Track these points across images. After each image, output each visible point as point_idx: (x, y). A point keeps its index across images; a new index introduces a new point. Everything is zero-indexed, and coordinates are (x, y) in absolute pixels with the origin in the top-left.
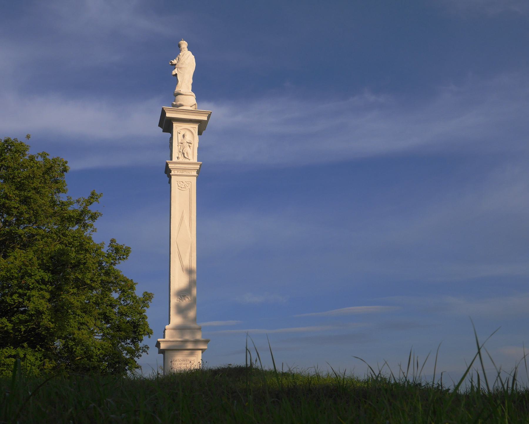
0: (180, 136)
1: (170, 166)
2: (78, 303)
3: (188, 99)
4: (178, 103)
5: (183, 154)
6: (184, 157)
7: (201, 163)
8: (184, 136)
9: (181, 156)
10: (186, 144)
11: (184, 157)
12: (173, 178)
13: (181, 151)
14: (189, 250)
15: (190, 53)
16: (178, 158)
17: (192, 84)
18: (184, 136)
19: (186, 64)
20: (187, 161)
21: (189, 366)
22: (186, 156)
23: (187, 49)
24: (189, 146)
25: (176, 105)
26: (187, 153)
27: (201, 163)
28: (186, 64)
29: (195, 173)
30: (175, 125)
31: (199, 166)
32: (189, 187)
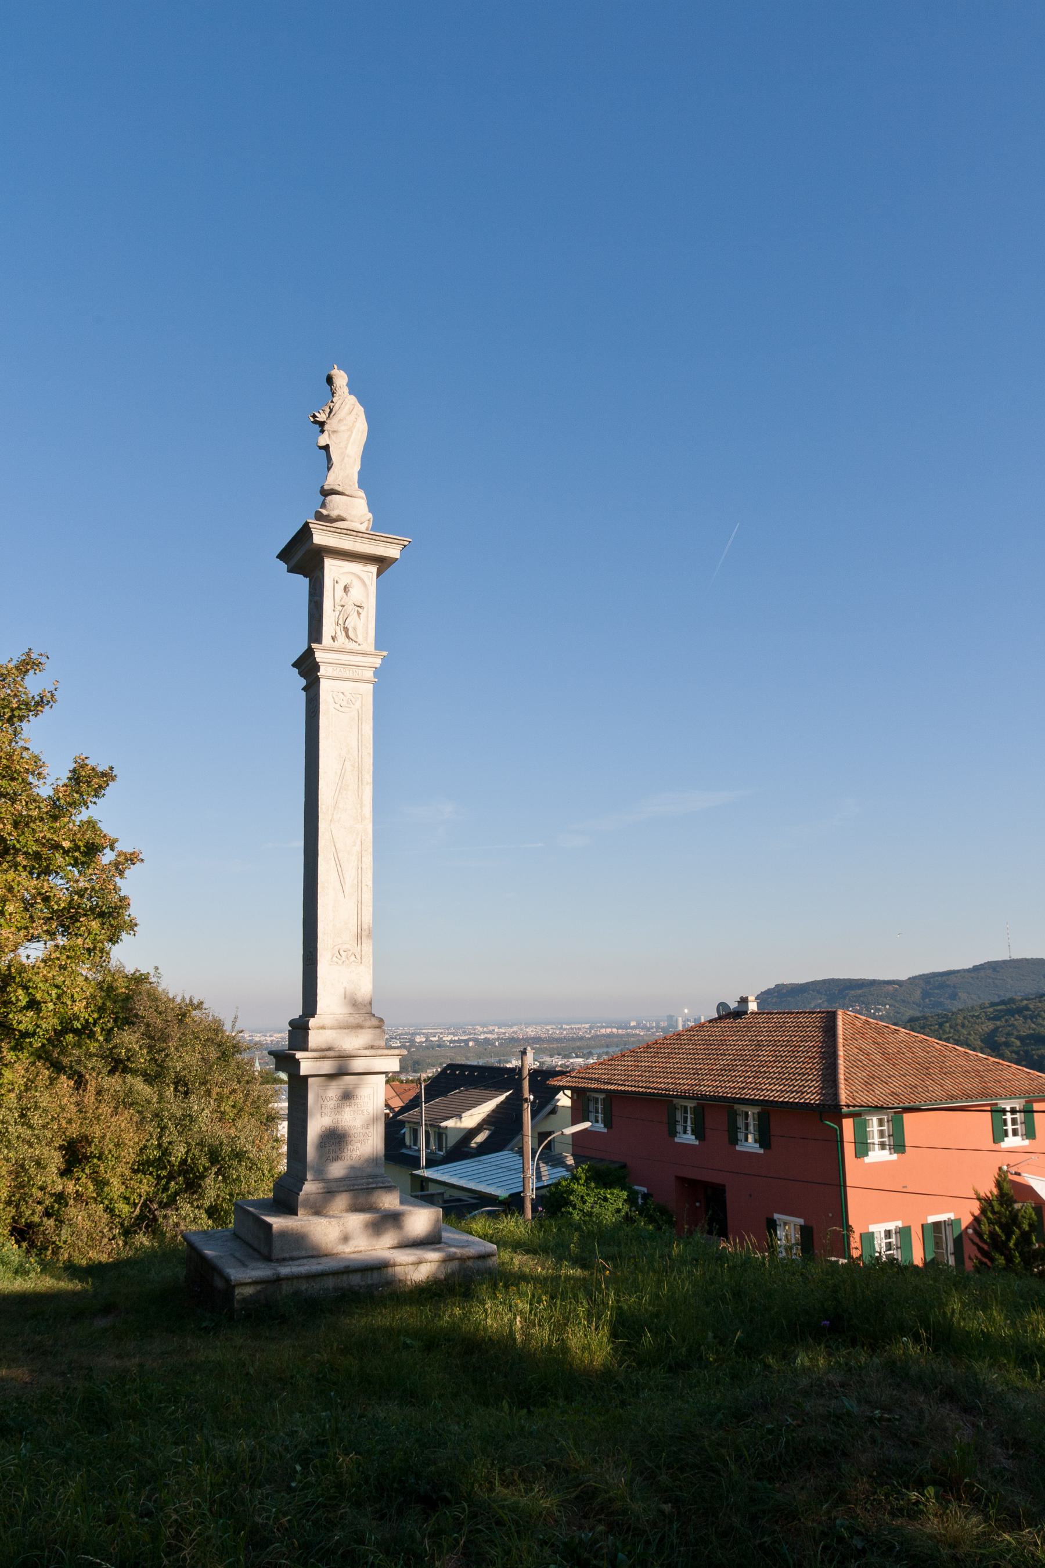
0: (340, 588)
1: (319, 656)
2: (124, 1120)
3: (354, 508)
4: (334, 514)
5: (346, 630)
6: (347, 636)
7: (385, 653)
8: (346, 589)
9: (341, 637)
10: (350, 608)
11: (347, 636)
12: (323, 683)
13: (341, 622)
14: (357, 848)
15: (352, 399)
16: (334, 638)
17: (359, 473)
18: (346, 589)
19: (349, 430)
20: (350, 646)
21: (11, 1287)
22: (351, 634)
23: (346, 390)
24: (359, 614)
25: (328, 516)
26: (355, 629)
27: (385, 653)
28: (349, 430)
29: (369, 674)
30: (329, 563)
31: (379, 661)
32: (358, 705)
